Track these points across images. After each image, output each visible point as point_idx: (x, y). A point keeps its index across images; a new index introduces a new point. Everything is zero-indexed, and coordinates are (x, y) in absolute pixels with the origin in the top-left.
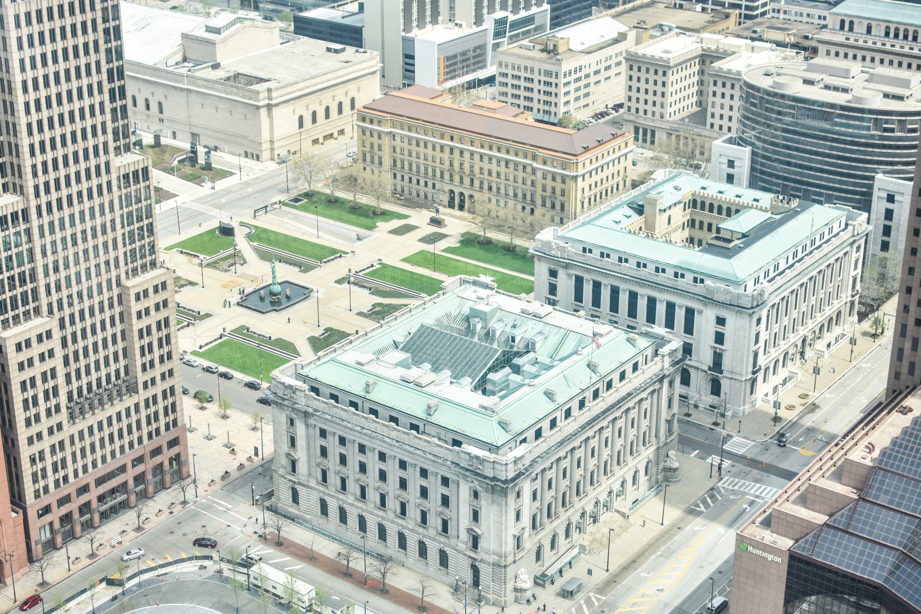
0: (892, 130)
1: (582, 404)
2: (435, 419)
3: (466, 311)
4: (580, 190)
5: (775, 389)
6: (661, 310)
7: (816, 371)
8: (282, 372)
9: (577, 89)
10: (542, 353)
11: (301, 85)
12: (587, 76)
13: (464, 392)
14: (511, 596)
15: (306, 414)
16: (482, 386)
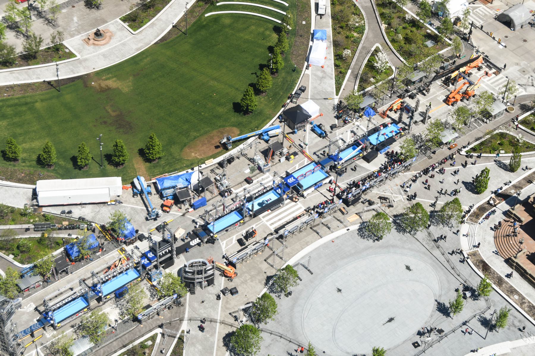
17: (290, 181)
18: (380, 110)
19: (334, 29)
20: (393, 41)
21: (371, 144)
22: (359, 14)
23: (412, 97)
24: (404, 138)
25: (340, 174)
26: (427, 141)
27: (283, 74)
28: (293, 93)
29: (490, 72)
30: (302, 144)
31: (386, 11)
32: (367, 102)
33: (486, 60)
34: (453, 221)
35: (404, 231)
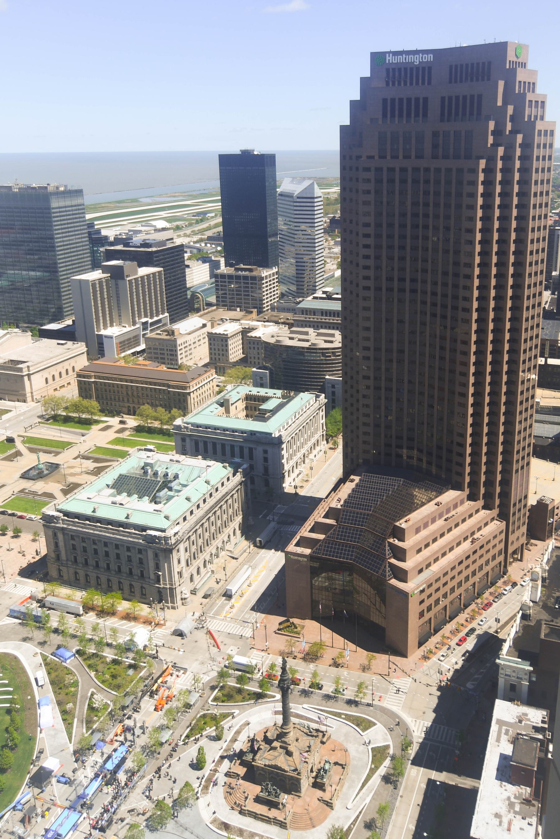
0: (330, 356)
1: (205, 501)
2: (132, 520)
3: (143, 465)
4: (193, 399)
5: (294, 480)
6: (237, 450)
7: (311, 468)
8: (47, 509)
9: (186, 352)
10: (182, 479)
11: (45, 363)
12: (190, 345)
13: (145, 504)
14: (179, 602)
15: (63, 529)
16: (155, 500)
17: (50, 835)
18: (108, 739)
19: (55, 692)
20: (103, 682)
21: (108, 770)
22: (70, 673)
23: (129, 718)
24: (133, 753)
25: (90, 807)
26: (152, 747)
27: (21, 747)
28: (34, 758)
29: (180, 674)
30: (53, 798)
31: (91, 662)
32: (98, 736)
33: (174, 666)
34: (191, 801)
35: (157, 829)
